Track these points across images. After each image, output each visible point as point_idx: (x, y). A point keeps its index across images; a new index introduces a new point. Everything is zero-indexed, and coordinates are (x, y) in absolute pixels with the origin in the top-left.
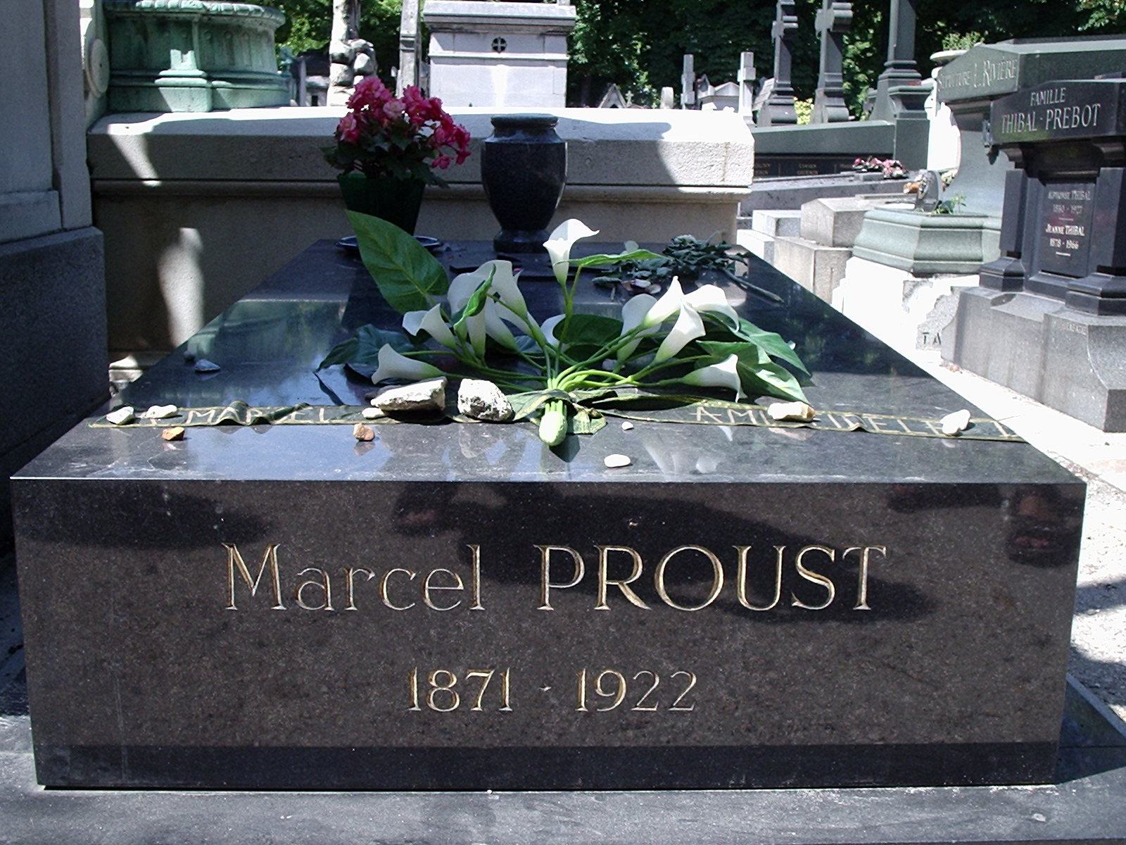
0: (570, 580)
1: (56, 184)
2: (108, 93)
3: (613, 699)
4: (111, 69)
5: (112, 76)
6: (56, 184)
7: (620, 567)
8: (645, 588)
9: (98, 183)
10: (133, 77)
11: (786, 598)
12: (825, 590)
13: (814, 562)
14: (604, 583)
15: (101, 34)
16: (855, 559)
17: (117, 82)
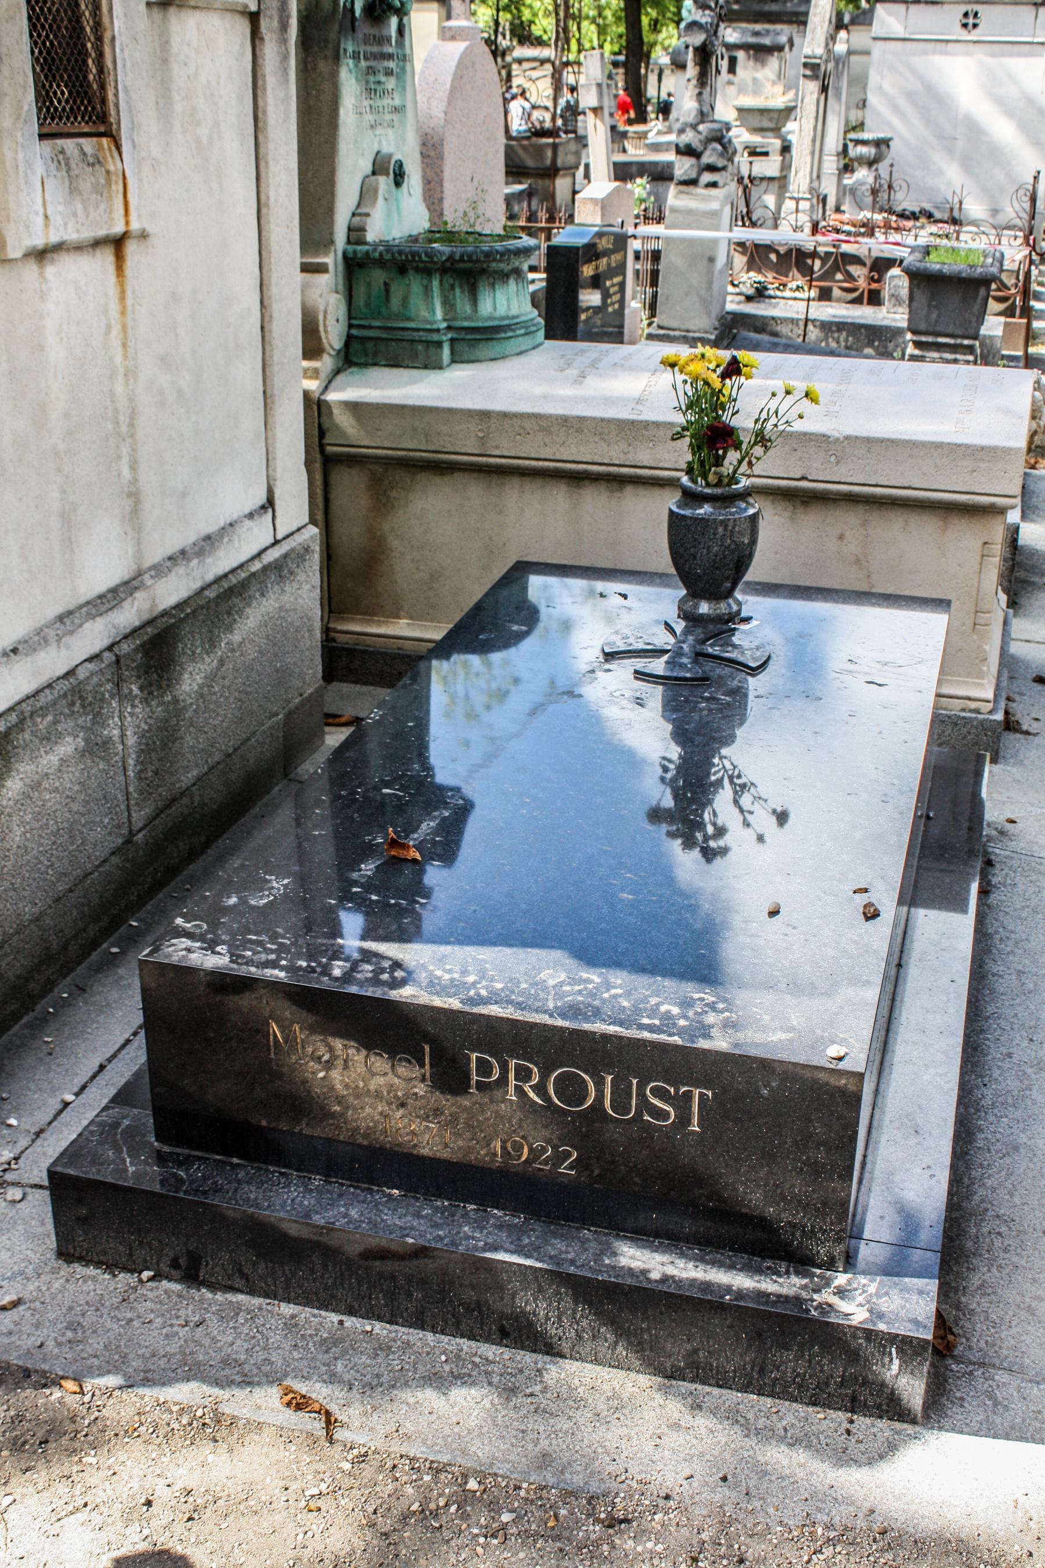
0: (490, 1076)
1: (270, 503)
2: (347, 344)
3: (520, 1157)
4: (350, 318)
5: (350, 326)
6: (270, 503)
7: (524, 1075)
8: (541, 1089)
9: (329, 448)
10: (370, 327)
11: (639, 1113)
12: (668, 1113)
13: (658, 1092)
14: (512, 1081)
15: (341, 287)
16: (688, 1096)
17: (354, 332)
